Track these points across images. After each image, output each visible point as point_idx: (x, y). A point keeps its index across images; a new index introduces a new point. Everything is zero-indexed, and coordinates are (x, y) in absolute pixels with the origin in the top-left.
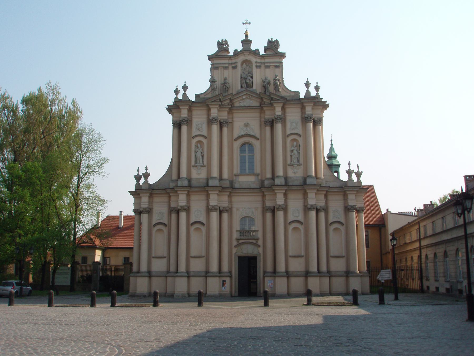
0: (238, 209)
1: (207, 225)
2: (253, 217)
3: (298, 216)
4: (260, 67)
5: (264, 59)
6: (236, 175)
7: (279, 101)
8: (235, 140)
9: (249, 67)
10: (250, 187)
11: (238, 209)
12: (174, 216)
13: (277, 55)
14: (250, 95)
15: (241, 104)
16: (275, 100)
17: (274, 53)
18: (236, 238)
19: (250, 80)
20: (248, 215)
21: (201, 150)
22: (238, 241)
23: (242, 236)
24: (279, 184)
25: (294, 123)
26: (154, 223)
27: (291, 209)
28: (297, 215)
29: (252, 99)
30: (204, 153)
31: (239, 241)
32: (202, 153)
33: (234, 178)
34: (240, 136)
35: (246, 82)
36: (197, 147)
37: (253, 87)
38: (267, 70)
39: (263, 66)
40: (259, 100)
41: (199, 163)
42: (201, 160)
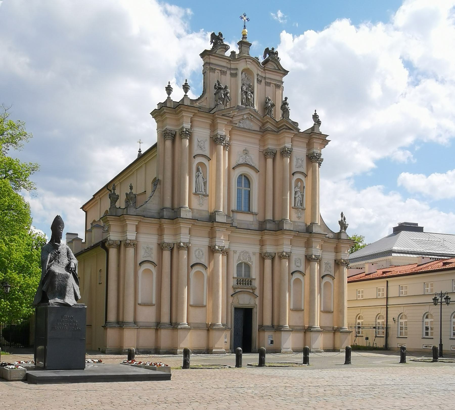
0: (235, 252)
1: (159, 265)
2: (251, 264)
3: (300, 266)
4: (261, 81)
5: (265, 73)
6: (233, 211)
7: (292, 132)
8: (233, 168)
9: (248, 78)
10: (248, 228)
11: (235, 252)
12: (166, 254)
13: (279, 71)
14: (252, 115)
15: (241, 125)
16: (288, 129)
17: (276, 69)
18: (233, 287)
19: (251, 96)
20: (244, 261)
21: (202, 174)
22: (234, 290)
23: (239, 284)
24: (288, 229)
25: (300, 160)
26: (141, 258)
27: (293, 258)
28: (299, 265)
29: (252, 121)
30: (206, 179)
31: (235, 290)
32: (203, 178)
33: (231, 213)
34: (239, 165)
35: (247, 99)
36: (198, 170)
37: (253, 105)
38: (268, 88)
39: (263, 81)
40: (260, 124)
41: (201, 191)
42: (203, 187)
